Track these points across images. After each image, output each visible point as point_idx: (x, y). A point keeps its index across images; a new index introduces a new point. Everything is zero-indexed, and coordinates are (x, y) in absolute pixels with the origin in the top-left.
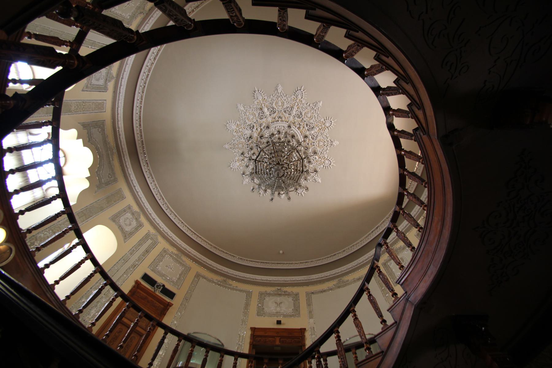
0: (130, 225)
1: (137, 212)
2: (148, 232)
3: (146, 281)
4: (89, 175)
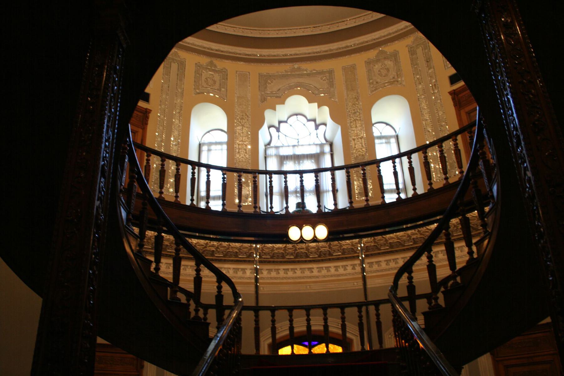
0: (388, 70)
1: (378, 53)
2: (407, 48)
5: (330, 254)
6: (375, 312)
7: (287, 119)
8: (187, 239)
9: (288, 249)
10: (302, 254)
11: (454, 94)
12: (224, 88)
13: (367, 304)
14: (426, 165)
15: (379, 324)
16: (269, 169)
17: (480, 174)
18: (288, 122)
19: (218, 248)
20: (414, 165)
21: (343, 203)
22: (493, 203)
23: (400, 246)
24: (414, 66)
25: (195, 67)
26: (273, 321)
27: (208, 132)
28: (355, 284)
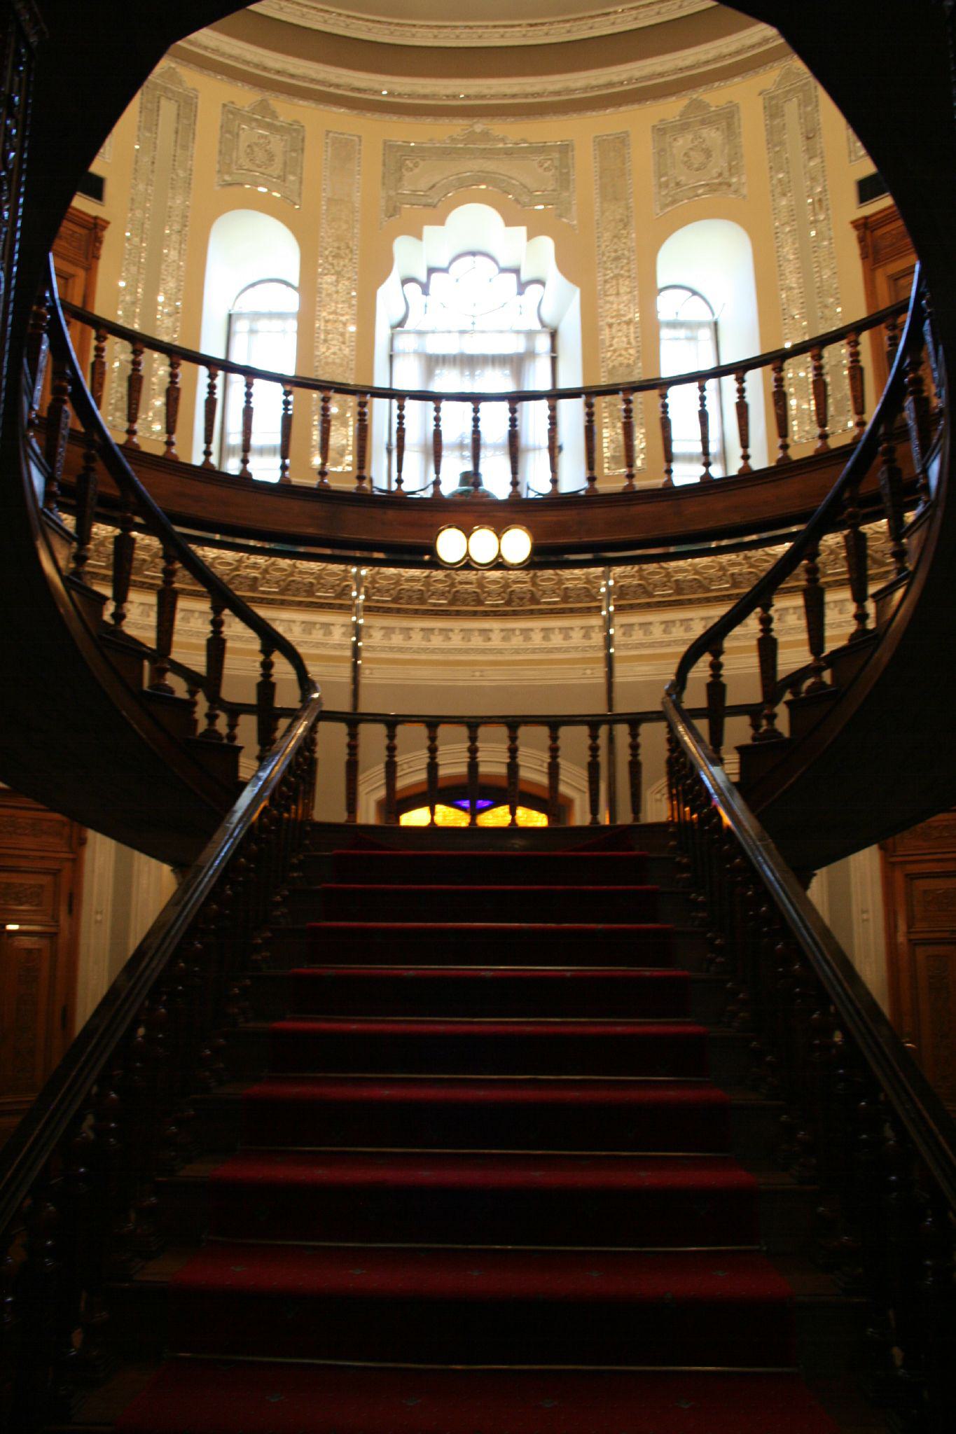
0: (708, 153)
1: (688, 107)
2: (761, 97)
3: (871, 198)
4: (522, 230)
5: (534, 600)
6: (628, 740)
7: (451, 263)
8: (193, 547)
9: (435, 581)
10: (466, 596)
11: (864, 227)
12: (294, 174)
13: (612, 720)
14: (779, 399)
15: (635, 767)
16: (398, 385)
17: (904, 433)
18: (451, 270)
19: (266, 571)
20: (749, 397)
21: (573, 480)
22: (926, 503)
23: (700, 590)
24: (775, 146)
25: (223, 113)
26: (391, 749)
27: (253, 285)
28: (589, 672)
